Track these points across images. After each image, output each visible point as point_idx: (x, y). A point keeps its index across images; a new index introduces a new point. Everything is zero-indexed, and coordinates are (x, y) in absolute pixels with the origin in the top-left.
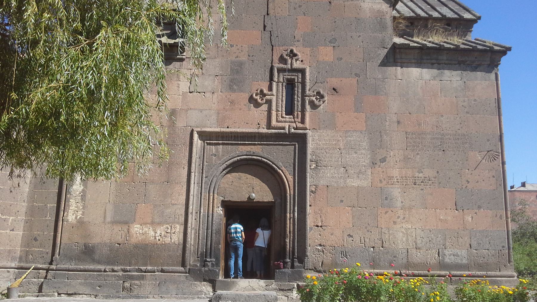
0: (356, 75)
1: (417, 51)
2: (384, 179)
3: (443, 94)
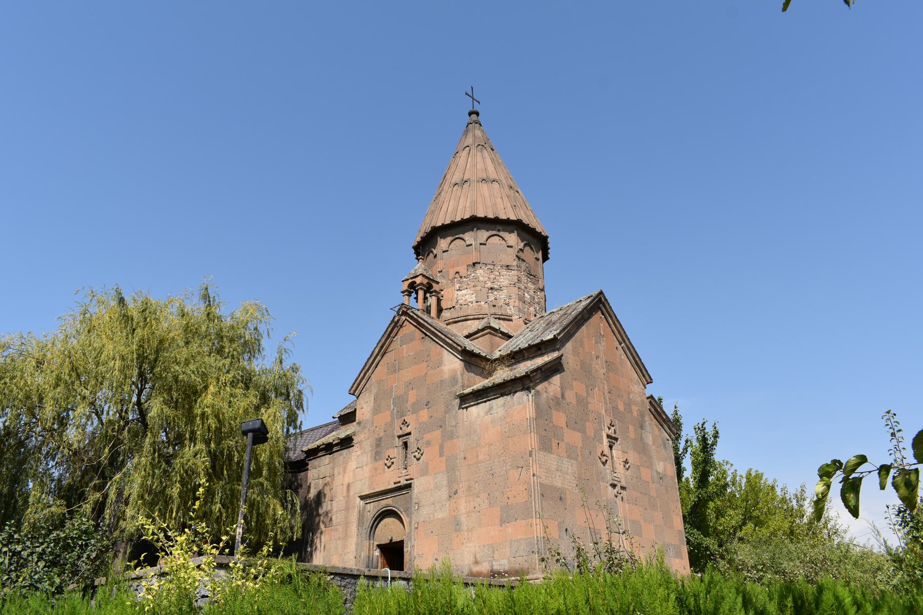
0: (441, 427)
1: (471, 396)
2: (456, 508)
3: (492, 425)
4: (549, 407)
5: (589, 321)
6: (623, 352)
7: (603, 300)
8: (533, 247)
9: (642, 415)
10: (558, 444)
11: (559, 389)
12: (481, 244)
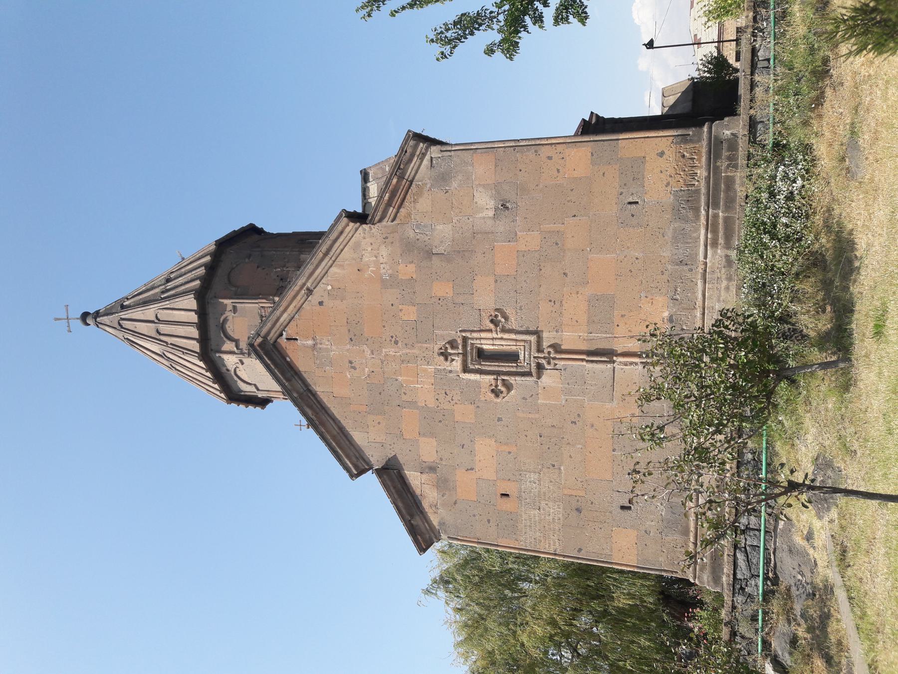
4: (455, 503)
5: (305, 375)
6: (321, 285)
7: (259, 340)
8: (222, 320)
9: (409, 248)
10: (503, 495)
11: (424, 476)
12: (258, 390)
